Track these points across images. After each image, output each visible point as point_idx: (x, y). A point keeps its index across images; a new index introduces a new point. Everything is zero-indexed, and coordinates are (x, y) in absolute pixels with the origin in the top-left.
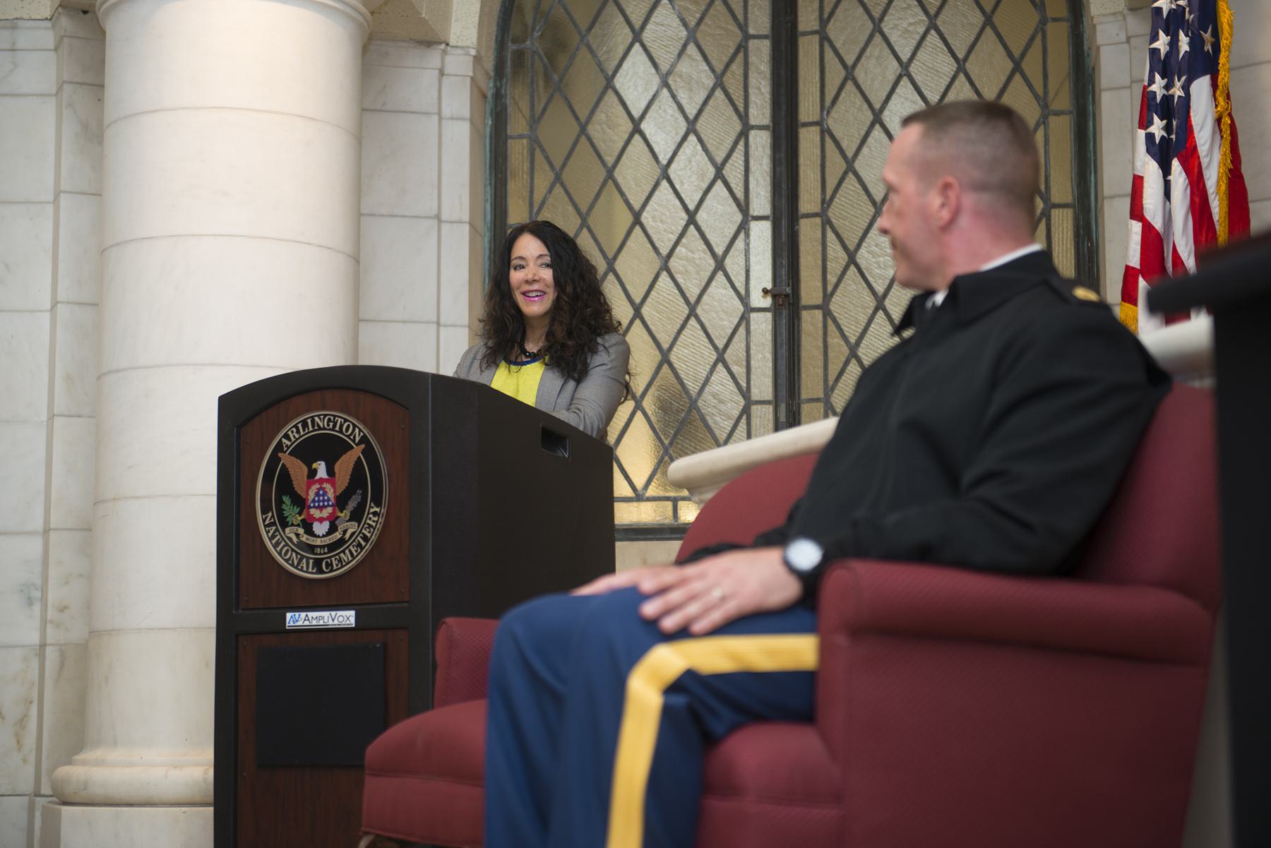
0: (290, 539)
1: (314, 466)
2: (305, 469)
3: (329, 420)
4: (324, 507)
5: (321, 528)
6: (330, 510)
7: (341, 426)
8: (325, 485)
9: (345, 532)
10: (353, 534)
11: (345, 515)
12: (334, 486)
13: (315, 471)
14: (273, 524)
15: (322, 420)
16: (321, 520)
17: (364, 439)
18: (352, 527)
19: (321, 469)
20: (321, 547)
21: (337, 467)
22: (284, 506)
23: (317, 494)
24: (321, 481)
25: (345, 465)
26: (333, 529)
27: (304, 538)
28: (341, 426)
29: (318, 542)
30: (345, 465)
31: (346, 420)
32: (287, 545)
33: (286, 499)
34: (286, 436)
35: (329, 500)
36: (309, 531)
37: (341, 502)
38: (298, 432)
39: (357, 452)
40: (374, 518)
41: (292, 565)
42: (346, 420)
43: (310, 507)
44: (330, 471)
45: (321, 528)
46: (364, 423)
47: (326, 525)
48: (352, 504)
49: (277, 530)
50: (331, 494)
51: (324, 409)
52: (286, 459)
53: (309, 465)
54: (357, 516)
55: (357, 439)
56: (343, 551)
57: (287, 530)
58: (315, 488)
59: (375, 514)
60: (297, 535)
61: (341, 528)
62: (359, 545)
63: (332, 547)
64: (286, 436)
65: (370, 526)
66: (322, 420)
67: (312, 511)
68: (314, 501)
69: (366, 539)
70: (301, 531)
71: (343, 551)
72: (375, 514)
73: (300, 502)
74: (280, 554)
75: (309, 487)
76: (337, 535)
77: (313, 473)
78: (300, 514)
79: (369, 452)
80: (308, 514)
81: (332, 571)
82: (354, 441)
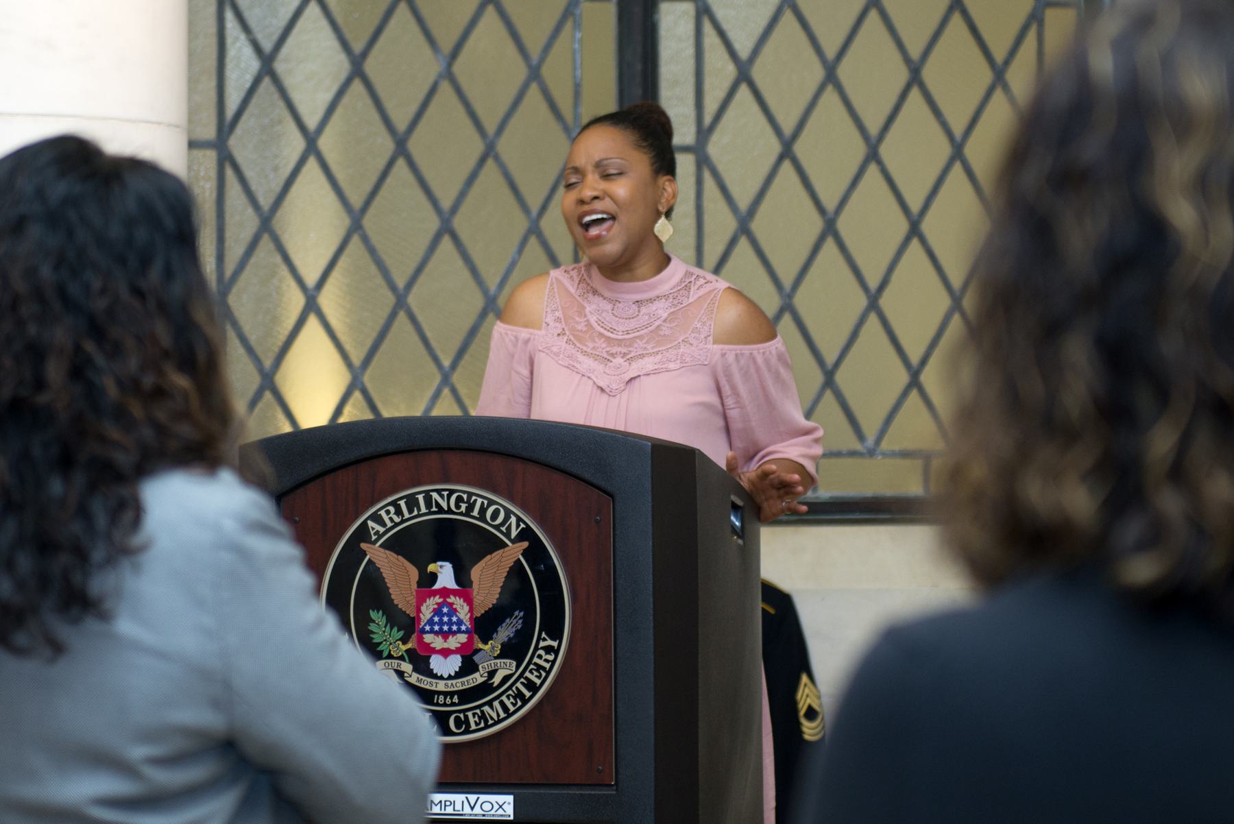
1: (431, 568)
2: (414, 573)
3: (459, 499)
4: (451, 633)
5: (445, 666)
6: (463, 638)
7: (483, 510)
8: (452, 599)
9: (492, 674)
10: (506, 679)
12: (469, 601)
13: (434, 577)
15: (445, 498)
16: (446, 653)
17: (526, 534)
18: (506, 668)
19: (445, 575)
20: (445, 694)
21: (476, 573)
22: (372, 627)
23: (438, 612)
24: (445, 592)
26: (468, 667)
28: (483, 510)
29: (441, 686)
31: (491, 502)
35: (460, 622)
36: (421, 665)
37: (485, 626)
38: (399, 512)
39: (514, 552)
40: (549, 659)
42: (491, 502)
43: (423, 631)
44: (461, 576)
45: (445, 666)
46: (524, 506)
47: (455, 663)
48: (505, 633)
51: (446, 480)
52: (375, 553)
54: (515, 650)
55: (514, 533)
56: (490, 703)
58: (430, 604)
59: (548, 650)
61: (484, 668)
62: (519, 695)
63: (467, 696)
65: (539, 667)
66: (445, 498)
67: (428, 638)
70: (407, 667)
71: (490, 703)
72: (548, 650)
73: (408, 626)
75: (420, 601)
76: (477, 678)
78: (404, 640)
79: (536, 552)
80: (420, 640)
81: (467, 731)
82: (508, 534)
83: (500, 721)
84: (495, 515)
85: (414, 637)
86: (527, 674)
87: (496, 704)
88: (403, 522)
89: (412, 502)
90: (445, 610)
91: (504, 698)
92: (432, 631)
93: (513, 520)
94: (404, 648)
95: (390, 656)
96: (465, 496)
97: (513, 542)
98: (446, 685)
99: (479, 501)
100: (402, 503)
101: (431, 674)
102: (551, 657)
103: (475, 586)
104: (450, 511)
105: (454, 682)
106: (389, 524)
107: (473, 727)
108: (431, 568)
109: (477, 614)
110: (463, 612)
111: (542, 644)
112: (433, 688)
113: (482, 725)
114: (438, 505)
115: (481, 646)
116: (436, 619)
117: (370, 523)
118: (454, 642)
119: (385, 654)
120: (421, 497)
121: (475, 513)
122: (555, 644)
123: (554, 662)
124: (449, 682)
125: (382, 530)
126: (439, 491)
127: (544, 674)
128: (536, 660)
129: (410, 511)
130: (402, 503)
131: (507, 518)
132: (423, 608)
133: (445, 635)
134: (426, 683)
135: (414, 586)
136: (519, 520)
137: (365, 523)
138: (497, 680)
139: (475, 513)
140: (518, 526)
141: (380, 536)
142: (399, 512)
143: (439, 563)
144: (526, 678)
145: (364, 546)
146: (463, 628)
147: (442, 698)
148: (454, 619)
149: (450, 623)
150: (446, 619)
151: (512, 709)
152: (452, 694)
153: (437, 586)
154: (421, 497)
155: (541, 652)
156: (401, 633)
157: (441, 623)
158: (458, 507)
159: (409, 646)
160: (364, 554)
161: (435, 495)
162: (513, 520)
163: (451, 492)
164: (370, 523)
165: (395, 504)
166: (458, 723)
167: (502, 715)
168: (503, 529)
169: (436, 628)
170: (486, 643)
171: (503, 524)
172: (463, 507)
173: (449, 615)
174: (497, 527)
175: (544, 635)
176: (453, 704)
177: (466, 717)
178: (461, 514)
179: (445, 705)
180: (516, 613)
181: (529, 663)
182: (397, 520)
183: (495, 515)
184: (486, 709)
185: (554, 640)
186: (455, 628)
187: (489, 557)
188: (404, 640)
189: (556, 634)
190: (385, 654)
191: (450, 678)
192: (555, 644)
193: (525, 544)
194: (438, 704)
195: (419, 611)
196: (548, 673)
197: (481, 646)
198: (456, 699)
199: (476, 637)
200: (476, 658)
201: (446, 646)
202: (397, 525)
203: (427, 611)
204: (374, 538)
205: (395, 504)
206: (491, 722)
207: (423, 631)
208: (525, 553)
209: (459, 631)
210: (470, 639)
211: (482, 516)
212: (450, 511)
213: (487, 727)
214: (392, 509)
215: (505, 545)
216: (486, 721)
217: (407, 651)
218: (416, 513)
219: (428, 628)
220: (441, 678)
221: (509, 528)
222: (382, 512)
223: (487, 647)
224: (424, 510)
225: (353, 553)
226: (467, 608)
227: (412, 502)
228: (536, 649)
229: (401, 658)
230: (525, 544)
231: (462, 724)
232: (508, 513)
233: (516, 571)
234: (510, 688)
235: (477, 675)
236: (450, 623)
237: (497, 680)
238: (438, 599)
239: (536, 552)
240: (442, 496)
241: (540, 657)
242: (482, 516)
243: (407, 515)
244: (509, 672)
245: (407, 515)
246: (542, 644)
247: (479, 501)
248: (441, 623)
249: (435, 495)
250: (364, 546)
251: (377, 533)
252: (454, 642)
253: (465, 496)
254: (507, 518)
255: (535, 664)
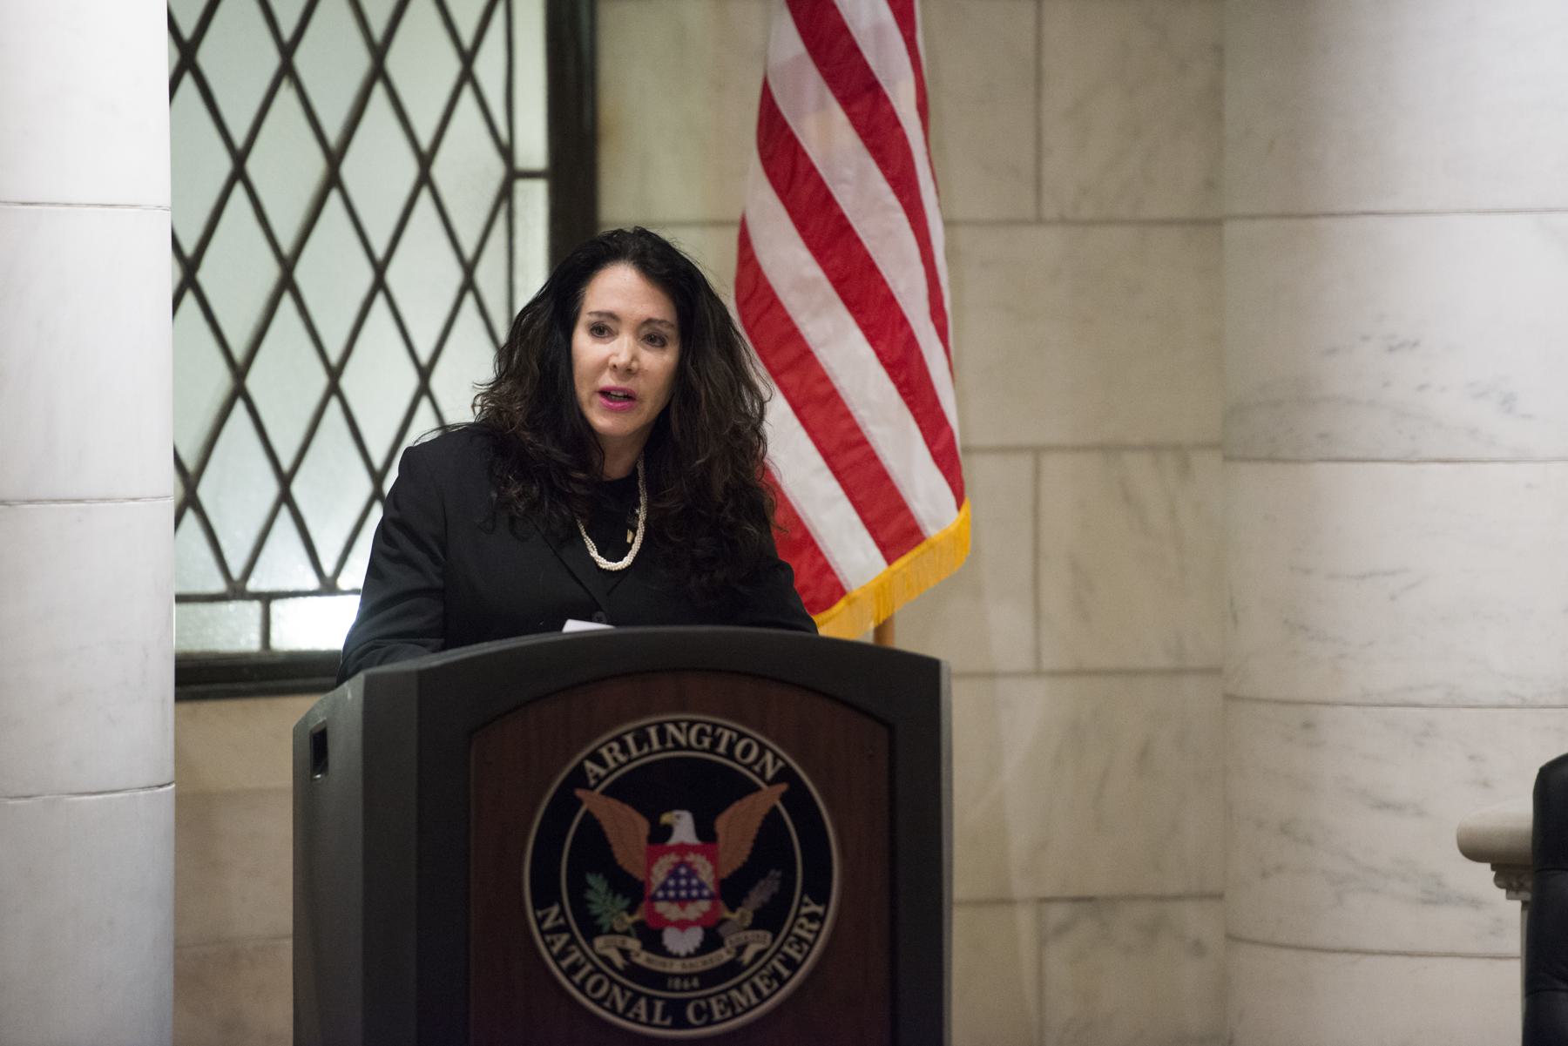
0: (607, 960)
1: (666, 818)
2: (643, 826)
3: (701, 733)
4: (690, 899)
5: (682, 941)
6: (704, 906)
8: (691, 858)
9: (741, 949)
10: (759, 955)
11: (744, 915)
12: (712, 858)
13: (668, 830)
14: (566, 928)
15: (684, 733)
16: (683, 925)
17: (785, 774)
18: (758, 942)
19: (683, 828)
20: (683, 977)
21: (721, 824)
22: (590, 895)
23: (673, 874)
24: (683, 849)
25: (739, 825)
26: (712, 941)
27: (642, 958)
28: (731, 746)
29: (677, 967)
30: (739, 825)
31: (742, 736)
32: (598, 970)
33: (597, 882)
34: (597, 758)
35: (701, 886)
36: (651, 938)
37: (732, 890)
38: (624, 749)
39: (770, 797)
40: (813, 930)
41: (613, 1010)
42: (742, 736)
43: (654, 899)
44: (705, 831)
45: (682, 941)
47: (695, 937)
48: (758, 896)
49: (573, 940)
50: (705, 872)
52: (593, 801)
53: (653, 817)
54: (770, 918)
55: (770, 773)
57: (599, 942)
59: (812, 917)
60: (625, 953)
61: (731, 941)
62: (776, 975)
63: (709, 978)
64: (597, 758)
65: (800, 940)
67: (661, 907)
68: (664, 887)
69: (792, 965)
70: (633, 944)
71: (738, 987)
72: (812, 917)
73: (632, 890)
74: (581, 987)
75: (652, 859)
76: (723, 956)
77: (660, 834)
79: (797, 799)
80: (651, 910)
81: (710, 1023)
82: (762, 775)
83: (751, 1008)
84: (747, 751)
85: (643, 905)
86: (786, 949)
87: (747, 987)
88: (630, 761)
89: (642, 738)
90: (683, 871)
91: (756, 980)
92: (666, 898)
93: (769, 757)
94: (630, 920)
95: (612, 932)
96: (709, 729)
97: (769, 783)
98: (684, 966)
99: (727, 734)
100: (629, 739)
101: (662, 951)
102: (815, 927)
103: (721, 839)
104: (689, 748)
105: (693, 961)
106: (612, 765)
107: (717, 1016)
108: (666, 818)
109: (726, 872)
110: (705, 872)
111: (805, 910)
112: (667, 970)
113: (729, 1014)
114: (674, 740)
115: (727, 914)
116: (672, 883)
117: (589, 765)
118: (694, 911)
119: (606, 928)
120: (653, 731)
121: (722, 748)
122: (820, 910)
123: (818, 933)
124: (688, 962)
125: (602, 772)
126: (676, 723)
127: (806, 947)
128: (797, 930)
129: (639, 748)
130: (629, 739)
131: (761, 755)
132: (655, 870)
133: (682, 902)
134: (657, 964)
135: (644, 842)
136: (776, 757)
137: (581, 766)
138: (748, 956)
139: (722, 748)
140: (775, 764)
141: (600, 779)
142: (624, 749)
143: (677, 813)
144: (785, 954)
145: (579, 793)
146: (706, 893)
147: (677, 984)
148: (694, 882)
149: (689, 887)
150: (683, 882)
151: (766, 992)
152: (689, 976)
153: (673, 841)
154: (653, 731)
155: (803, 920)
156: (626, 903)
157: (677, 888)
158: (699, 741)
159: (637, 917)
160: (579, 803)
161: (671, 728)
162: (769, 757)
163: (692, 723)
164: (589, 765)
165: (619, 739)
166: (699, 1013)
167: (754, 1000)
168: (757, 768)
169: (672, 894)
170: (733, 910)
171: (756, 762)
172: (707, 742)
173: (689, 876)
174: (749, 767)
175: (806, 899)
176: (692, 989)
177: (709, 1005)
178: (704, 750)
179: (682, 990)
180: (772, 872)
181: (789, 933)
182: (622, 758)
183: (747, 751)
184: (734, 993)
185: (818, 903)
186: (695, 893)
187: (737, 804)
188: (631, 910)
189: (822, 898)
190: (606, 928)
191: (689, 956)
192: (820, 910)
193: (783, 787)
194: (673, 990)
195: (649, 872)
196: (811, 946)
197: (727, 914)
198: (696, 983)
199: (721, 904)
200: (722, 930)
201: (683, 915)
202: (621, 765)
203: (659, 873)
204: (592, 782)
205: (619, 739)
206: (739, 1010)
207: (654, 899)
208: (784, 798)
209: (700, 897)
210: (714, 908)
211: (730, 753)
212: (689, 748)
213: (735, 1016)
214: (615, 746)
215: (757, 789)
216: (733, 1009)
217: (637, 925)
218: (646, 750)
219: (660, 894)
220: (677, 956)
221: (763, 768)
222: (604, 751)
223: (735, 916)
224: (656, 745)
225: (565, 803)
226: (709, 868)
227: (642, 738)
228: (797, 916)
229: (627, 933)
230: (783, 787)
231: (705, 1015)
232: (763, 748)
233: (772, 820)
234: (763, 966)
235: (722, 952)
236: (689, 887)
237: (748, 956)
238: (674, 858)
239: (797, 799)
240: (680, 729)
241: (801, 926)
242: (730, 753)
243: (634, 753)
244: (760, 947)
245: (634, 753)
246: (805, 910)
247: (727, 734)
248: (677, 888)
249: (671, 728)
250: (579, 793)
251: (597, 776)
252: (694, 911)
253: (709, 729)
254: (761, 755)
255: (797, 936)
